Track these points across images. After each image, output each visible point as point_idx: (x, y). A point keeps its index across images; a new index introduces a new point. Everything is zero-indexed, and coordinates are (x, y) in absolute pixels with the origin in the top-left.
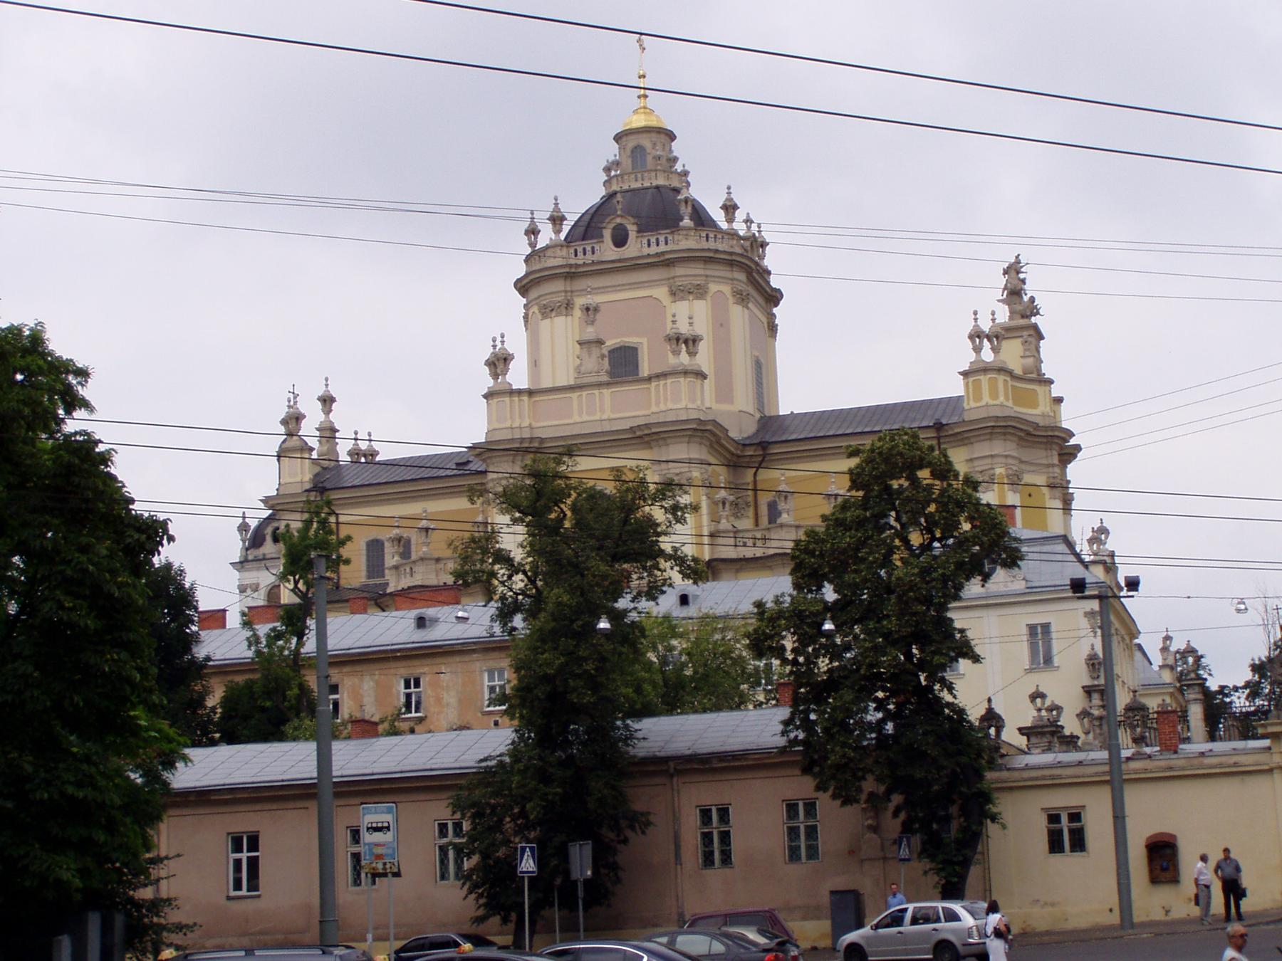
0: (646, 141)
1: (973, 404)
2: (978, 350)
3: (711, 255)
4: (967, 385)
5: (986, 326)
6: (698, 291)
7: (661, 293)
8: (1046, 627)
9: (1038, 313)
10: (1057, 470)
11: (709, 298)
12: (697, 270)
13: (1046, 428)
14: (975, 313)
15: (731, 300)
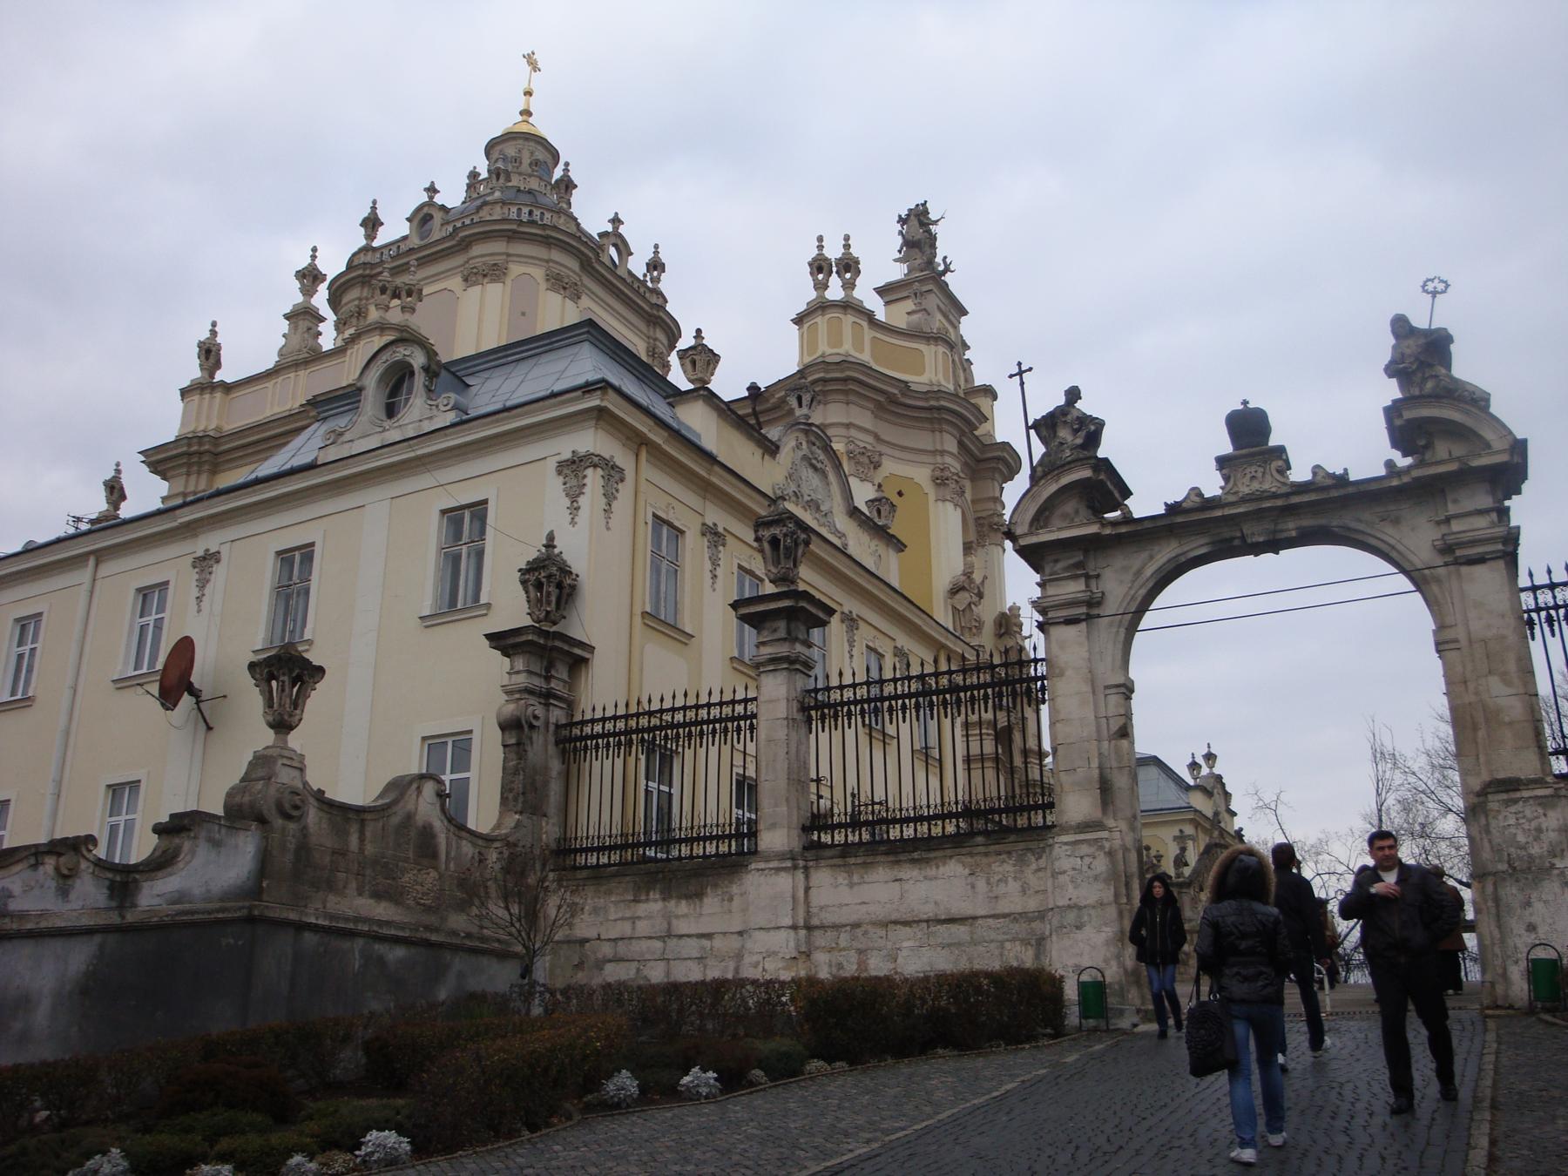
0: (510, 150)
1: (807, 360)
2: (821, 286)
3: (514, 227)
4: (802, 336)
5: (833, 252)
6: (495, 272)
7: (455, 283)
8: (479, 509)
9: (947, 269)
10: (955, 465)
11: (508, 281)
12: (498, 246)
13: (927, 395)
14: (820, 239)
15: (543, 285)
